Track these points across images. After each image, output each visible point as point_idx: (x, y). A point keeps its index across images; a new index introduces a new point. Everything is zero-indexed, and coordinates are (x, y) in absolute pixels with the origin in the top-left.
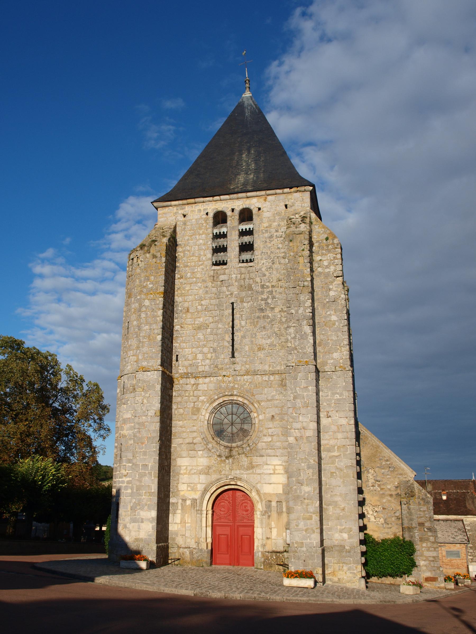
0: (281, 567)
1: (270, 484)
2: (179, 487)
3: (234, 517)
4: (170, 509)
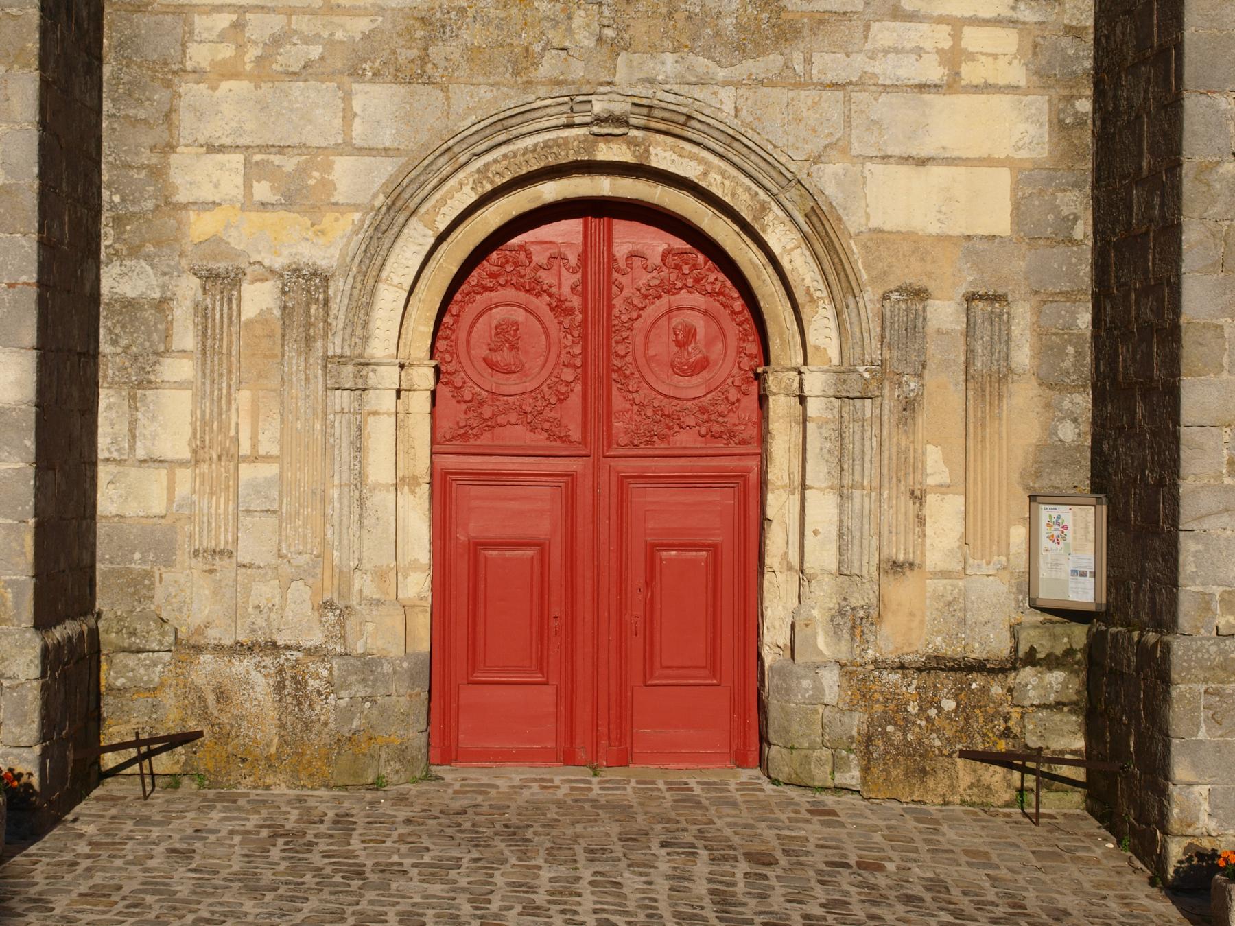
0: (995, 775)
1: (922, 162)
2: (177, 177)
3: (598, 415)
4: (105, 347)
